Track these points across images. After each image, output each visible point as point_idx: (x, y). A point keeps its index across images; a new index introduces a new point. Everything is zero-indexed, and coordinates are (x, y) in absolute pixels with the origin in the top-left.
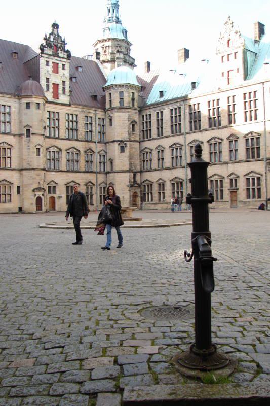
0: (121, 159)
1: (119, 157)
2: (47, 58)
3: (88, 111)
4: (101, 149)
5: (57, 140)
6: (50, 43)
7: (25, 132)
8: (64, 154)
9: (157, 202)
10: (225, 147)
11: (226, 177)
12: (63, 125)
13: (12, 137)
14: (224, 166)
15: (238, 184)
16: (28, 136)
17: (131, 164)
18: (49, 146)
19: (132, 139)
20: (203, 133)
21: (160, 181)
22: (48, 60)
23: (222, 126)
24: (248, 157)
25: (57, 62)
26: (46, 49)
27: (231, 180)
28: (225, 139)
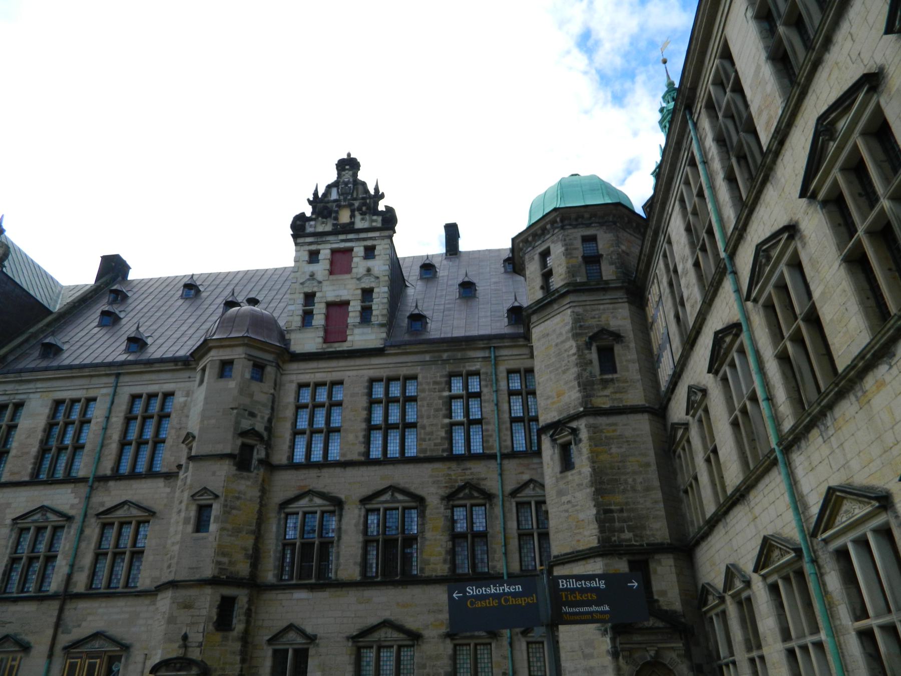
0: (565, 499)
1: (560, 493)
2: (311, 243)
3: (459, 355)
4: (526, 477)
5: (326, 472)
6: (326, 208)
8: (352, 516)
12: (349, 418)
13: (160, 483)
17: (605, 517)
18: (290, 494)
19: (603, 400)
22: (314, 247)
25: (342, 245)
26: (312, 223)
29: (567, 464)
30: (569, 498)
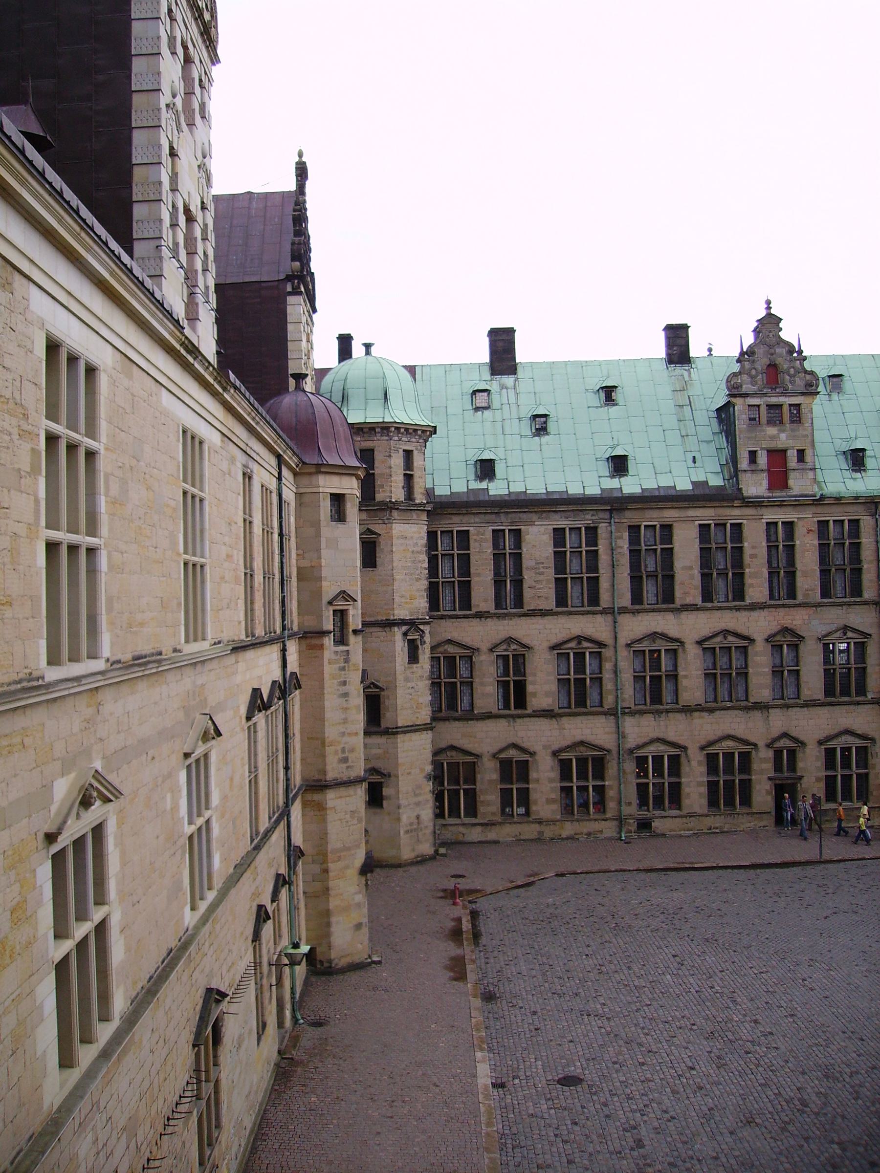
0: (410, 685)
1: (407, 680)
7: (328, 625)
9: (498, 818)
10: (761, 662)
11: (761, 744)
14: (757, 714)
15: (800, 765)
16: (342, 640)
20: (684, 615)
21: (512, 753)
23: (748, 601)
24: (829, 691)
27: (778, 753)
28: (759, 638)
29: (413, 658)
30: (413, 684)
